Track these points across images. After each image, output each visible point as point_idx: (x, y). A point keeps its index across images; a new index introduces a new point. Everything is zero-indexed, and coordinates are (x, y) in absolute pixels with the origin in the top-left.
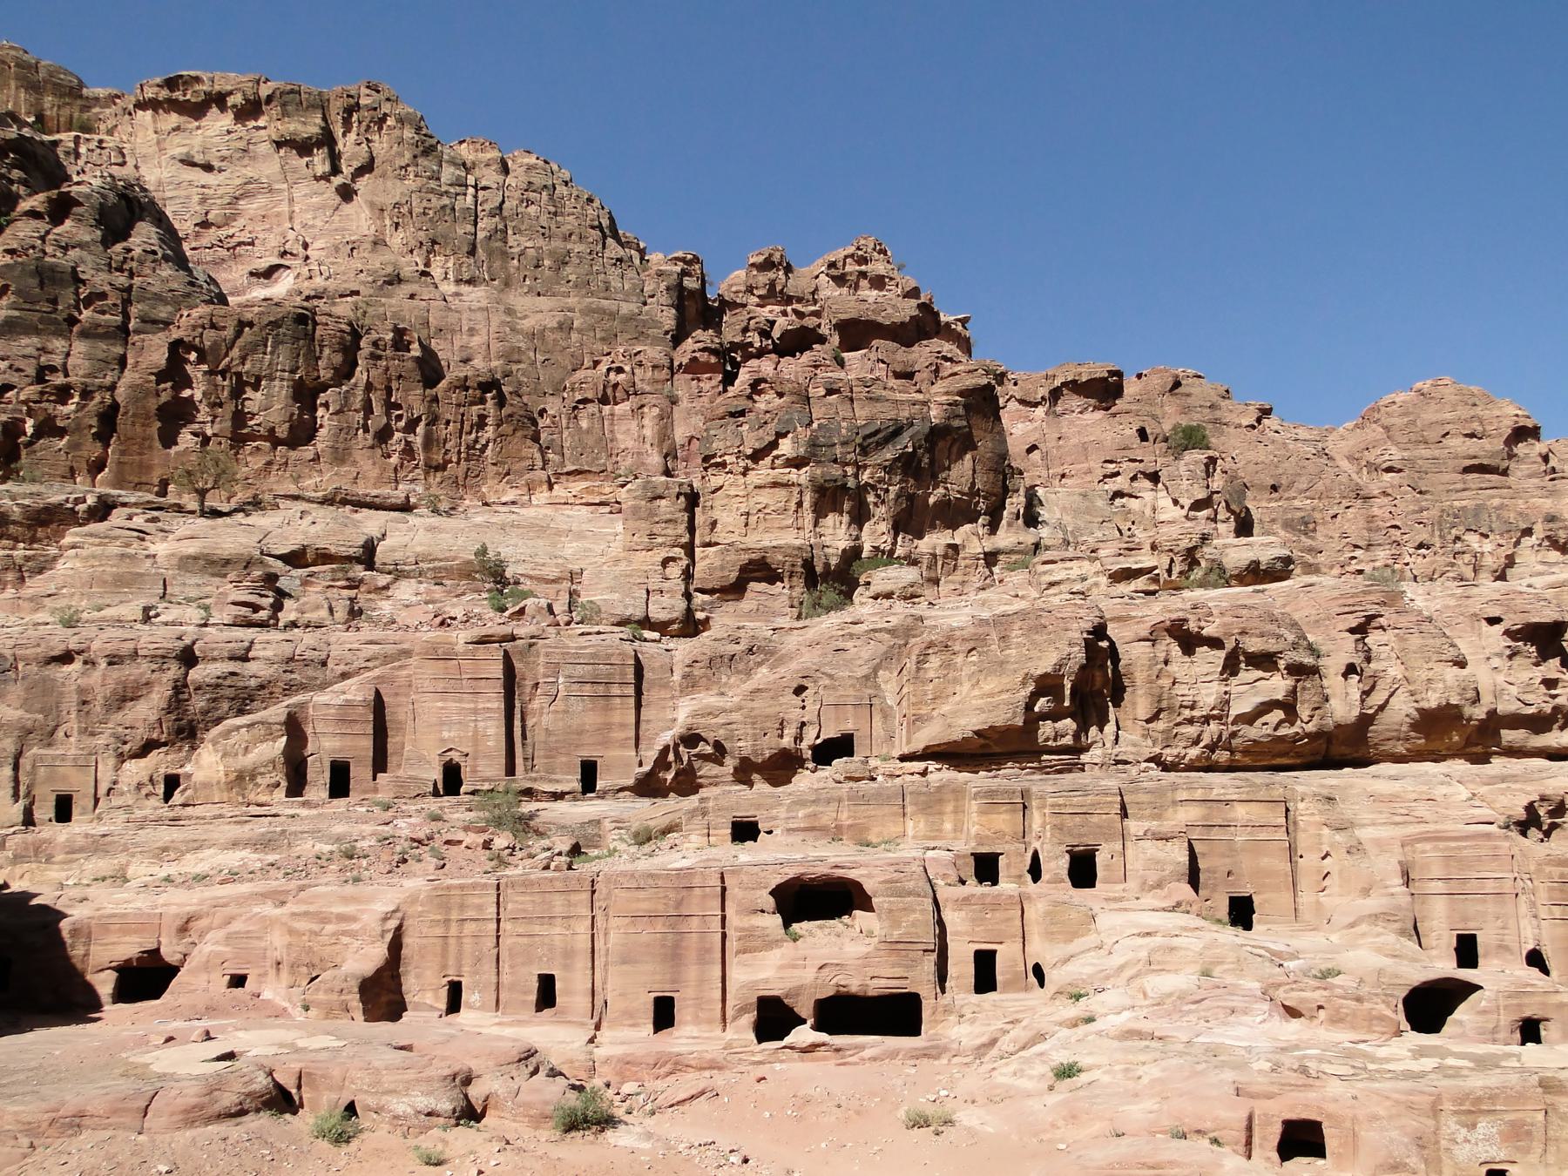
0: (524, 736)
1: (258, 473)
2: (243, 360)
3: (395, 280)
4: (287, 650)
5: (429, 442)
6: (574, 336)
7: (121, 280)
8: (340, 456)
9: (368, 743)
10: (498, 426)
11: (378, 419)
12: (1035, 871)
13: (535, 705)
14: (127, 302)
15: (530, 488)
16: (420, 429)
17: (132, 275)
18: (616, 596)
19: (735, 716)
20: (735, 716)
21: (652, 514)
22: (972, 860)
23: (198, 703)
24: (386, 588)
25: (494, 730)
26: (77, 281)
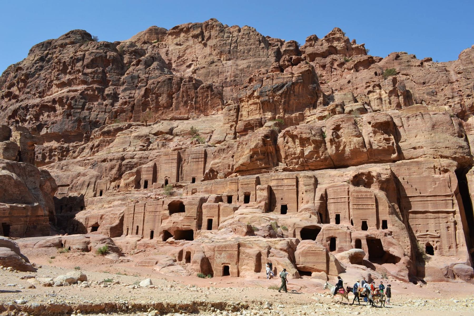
0: (181, 173)
1: (160, 115)
2: (158, 90)
3: (213, 62)
4: (140, 156)
5: (196, 103)
6: (251, 69)
7: (147, 75)
8: (177, 108)
9: (151, 176)
10: (211, 96)
11: (185, 99)
12: (238, 199)
13: (184, 165)
14: (148, 80)
15: (218, 111)
16: (194, 100)
17: (149, 74)
18: (219, 136)
19: (220, 164)
20: (220, 164)
21: (229, 114)
22: (226, 197)
23: (123, 169)
24: (172, 139)
25: (174, 171)
26: (139, 77)
